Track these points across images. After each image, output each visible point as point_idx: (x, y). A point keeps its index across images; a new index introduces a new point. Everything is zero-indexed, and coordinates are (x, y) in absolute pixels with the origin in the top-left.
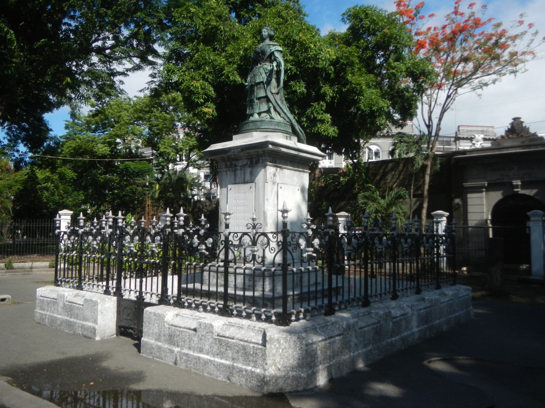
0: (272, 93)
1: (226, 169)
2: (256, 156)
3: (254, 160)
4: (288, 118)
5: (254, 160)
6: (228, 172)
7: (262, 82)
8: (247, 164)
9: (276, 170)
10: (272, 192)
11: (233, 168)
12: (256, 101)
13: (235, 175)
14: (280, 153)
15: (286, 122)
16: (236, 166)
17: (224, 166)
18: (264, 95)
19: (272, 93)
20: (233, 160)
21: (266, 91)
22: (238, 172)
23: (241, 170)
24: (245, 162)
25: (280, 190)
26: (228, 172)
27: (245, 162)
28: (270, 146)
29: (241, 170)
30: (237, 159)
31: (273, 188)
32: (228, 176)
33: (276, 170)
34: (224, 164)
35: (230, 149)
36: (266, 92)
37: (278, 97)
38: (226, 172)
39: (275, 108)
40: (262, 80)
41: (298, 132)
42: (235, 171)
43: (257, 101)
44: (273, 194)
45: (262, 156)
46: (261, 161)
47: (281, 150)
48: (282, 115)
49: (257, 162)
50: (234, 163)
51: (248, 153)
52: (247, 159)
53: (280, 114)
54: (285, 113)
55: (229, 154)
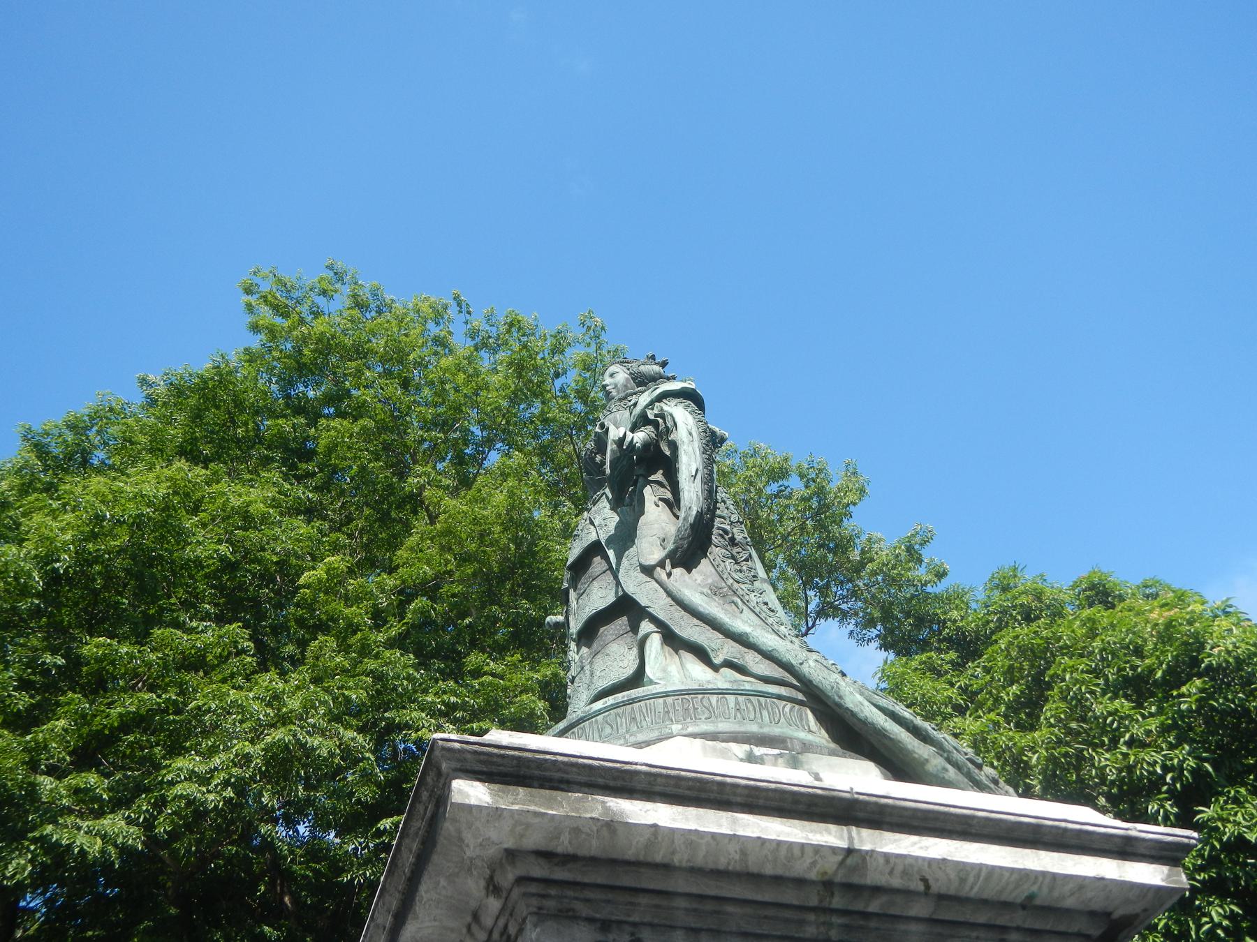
0: (648, 570)
4: (768, 656)
7: (595, 549)
14: (666, 868)
15: (748, 684)
18: (611, 598)
19: (648, 570)
21: (616, 577)
28: (470, 792)
36: (618, 583)
37: (693, 585)
39: (672, 640)
40: (593, 537)
41: (881, 734)
43: (584, 650)
47: (612, 826)
48: (724, 650)
53: (701, 654)
54: (742, 640)
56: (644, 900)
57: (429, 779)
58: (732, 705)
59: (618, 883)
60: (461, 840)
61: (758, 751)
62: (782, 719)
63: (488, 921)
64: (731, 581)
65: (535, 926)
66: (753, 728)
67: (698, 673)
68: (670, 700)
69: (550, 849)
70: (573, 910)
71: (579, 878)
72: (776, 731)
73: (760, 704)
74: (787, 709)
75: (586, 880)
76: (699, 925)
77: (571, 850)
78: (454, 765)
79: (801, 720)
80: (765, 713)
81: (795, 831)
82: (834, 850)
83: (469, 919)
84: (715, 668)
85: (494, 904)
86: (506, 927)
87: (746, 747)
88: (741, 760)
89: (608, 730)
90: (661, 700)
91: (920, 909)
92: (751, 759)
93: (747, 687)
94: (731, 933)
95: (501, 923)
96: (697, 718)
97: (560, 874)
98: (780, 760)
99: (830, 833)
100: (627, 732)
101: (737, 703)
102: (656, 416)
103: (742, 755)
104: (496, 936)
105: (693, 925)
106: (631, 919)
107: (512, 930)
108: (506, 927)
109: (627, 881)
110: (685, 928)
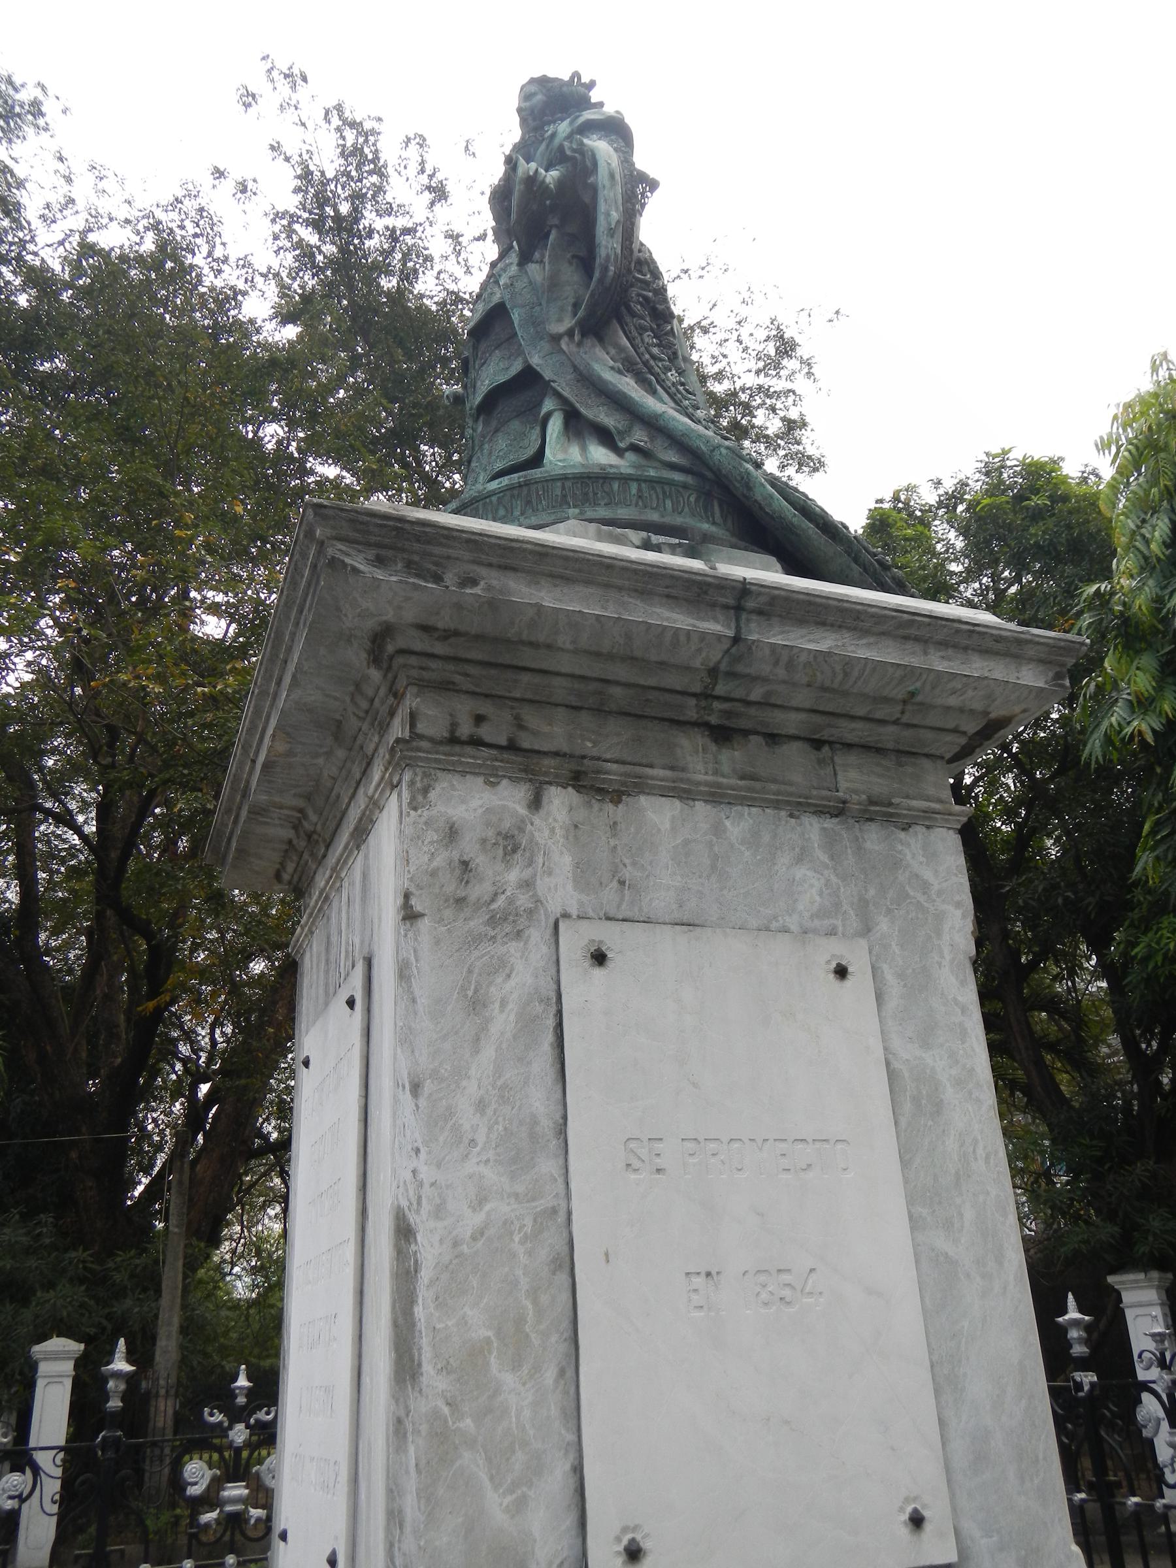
9: (536, 803)
10: (476, 1004)
25: (583, 989)
31: (501, 966)
33: (536, 803)
41: (789, 528)
44: (503, 1022)
53: (606, 437)
56: (526, 678)
58: (634, 491)
59: (500, 661)
60: (338, 609)
61: (656, 539)
62: (686, 509)
64: (647, 356)
65: (417, 696)
66: (654, 517)
67: (600, 455)
68: (568, 484)
69: (430, 623)
70: (454, 683)
71: (462, 654)
72: (678, 520)
73: (664, 493)
74: (692, 499)
75: (469, 656)
76: (579, 704)
77: (452, 626)
78: (329, 532)
79: (706, 512)
80: (669, 503)
81: (680, 617)
82: (719, 638)
83: (352, 688)
84: (619, 452)
87: (644, 534)
88: (638, 547)
89: (502, 512)
90: (559, 484)
91: (802, 698)
92: (647, 546)
93: (652, 473)
94: (610, 712)
96: (596, 504)
97: (439, 649)
98: (679, 550)
99: (718, 622)
100: (522, 514)
101: (640, 490)
102: (574, 151)
103: (638, 543)
105: (574, 704)
106: (512, 695)
109: (507, 659)
110: (567, 706)
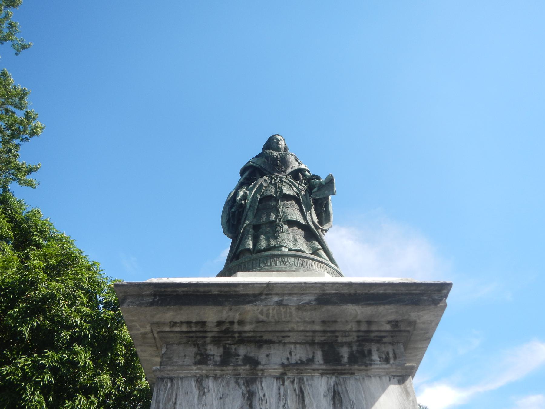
1: (204, 370)
2: (353, 337)
3: (345, 352)
5: (345, 352)
6: (210, 383)
8: (311, 361)
11: (244, 370)
12: (286, 227)
13: (250, 396)
16: (253, 362)
17: (189, 360)
20: (243, 341)
22: (268, 388)
23: (281, 378)
24: (300, 353)
26: (210, 383)
27: (300, 353)
29: (281, 378)
30: (260, 342)
32: (212, 398)
34: (191, 351)
35: (268, 289)
38: (199, 381)
42: (251, 380)
45: (379, 340)
46: (375, 357)
49: (360, 358)
50: (242, 351)
51: (324, 322)
52: (312, 343)
55: (251, 311)
57: (432, 288)
63: (374, 328)
85: (388, 327)
86: (384, 337)
95: (383, 334)
104: (373, 335)
107: (385, 340)
108: (384, 337)
